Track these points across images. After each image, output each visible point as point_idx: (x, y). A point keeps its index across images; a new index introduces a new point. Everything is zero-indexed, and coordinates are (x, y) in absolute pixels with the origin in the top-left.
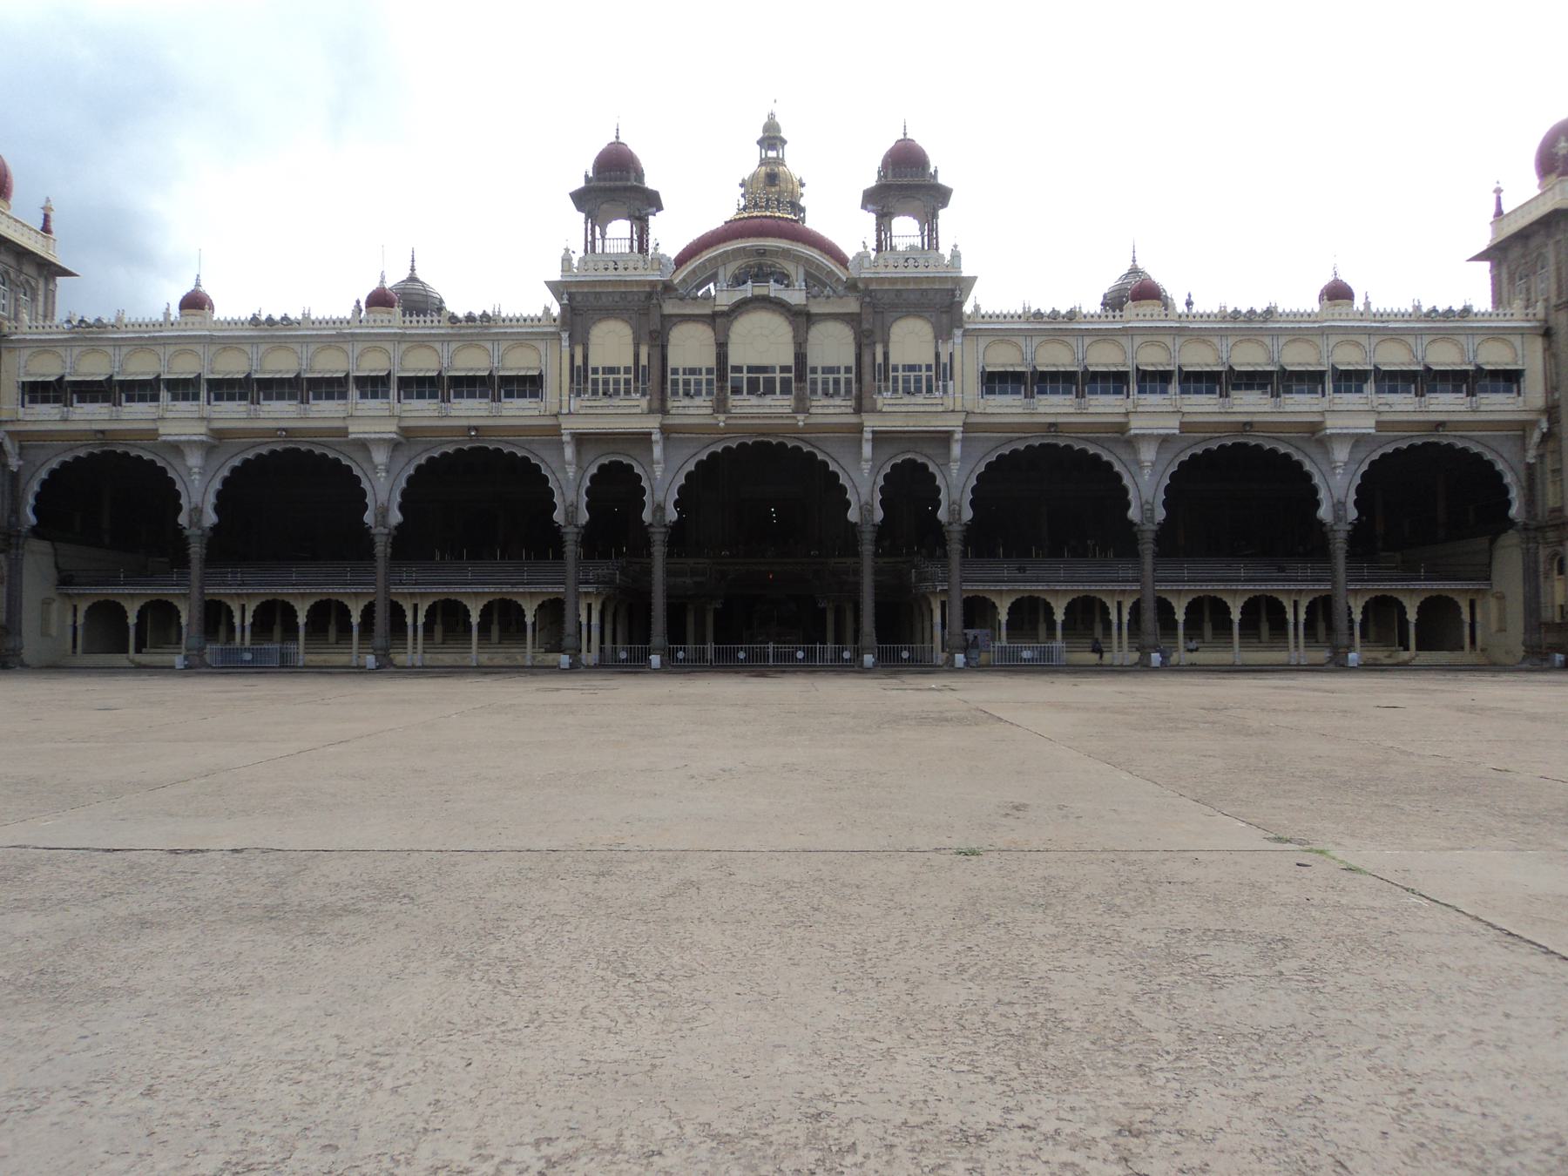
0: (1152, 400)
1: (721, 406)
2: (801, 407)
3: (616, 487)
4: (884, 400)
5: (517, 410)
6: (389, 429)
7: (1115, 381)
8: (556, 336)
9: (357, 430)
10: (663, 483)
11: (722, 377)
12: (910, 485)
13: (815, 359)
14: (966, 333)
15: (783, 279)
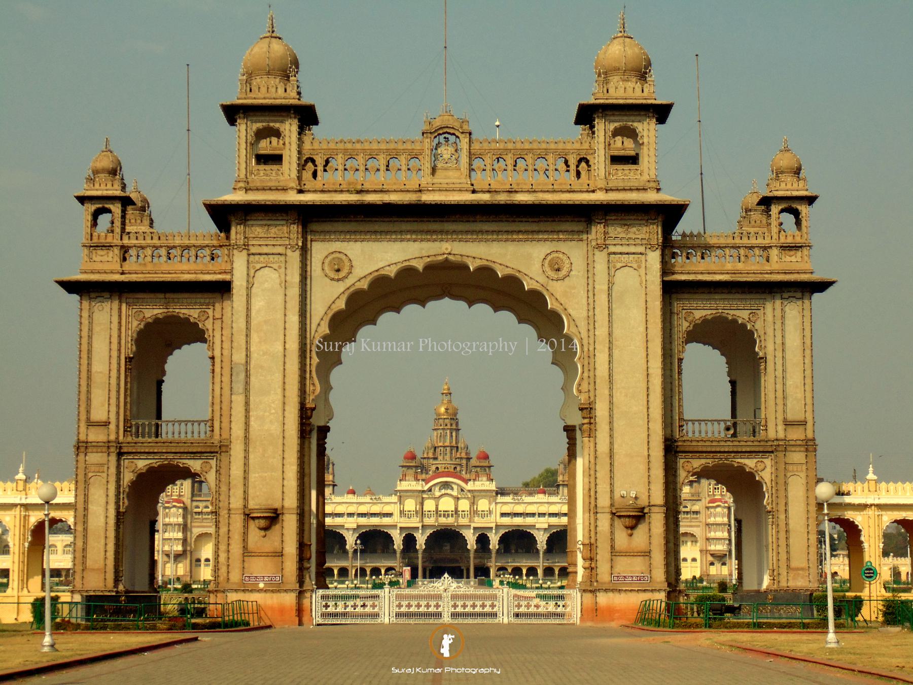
0: (542, 519)
1: (437, 520)
2: (457, 520)
3: (409, 540)
4: (476, 519)
5: (386, 521)
6: (355, 526)
7: (533, 515)
8: (395, 503)
9: (347, 526)
10: (421, 540)
11: (437, 513)
12: (483, 540)
13: (460, 509)
14: (496, 503)
15: (452, 489)
